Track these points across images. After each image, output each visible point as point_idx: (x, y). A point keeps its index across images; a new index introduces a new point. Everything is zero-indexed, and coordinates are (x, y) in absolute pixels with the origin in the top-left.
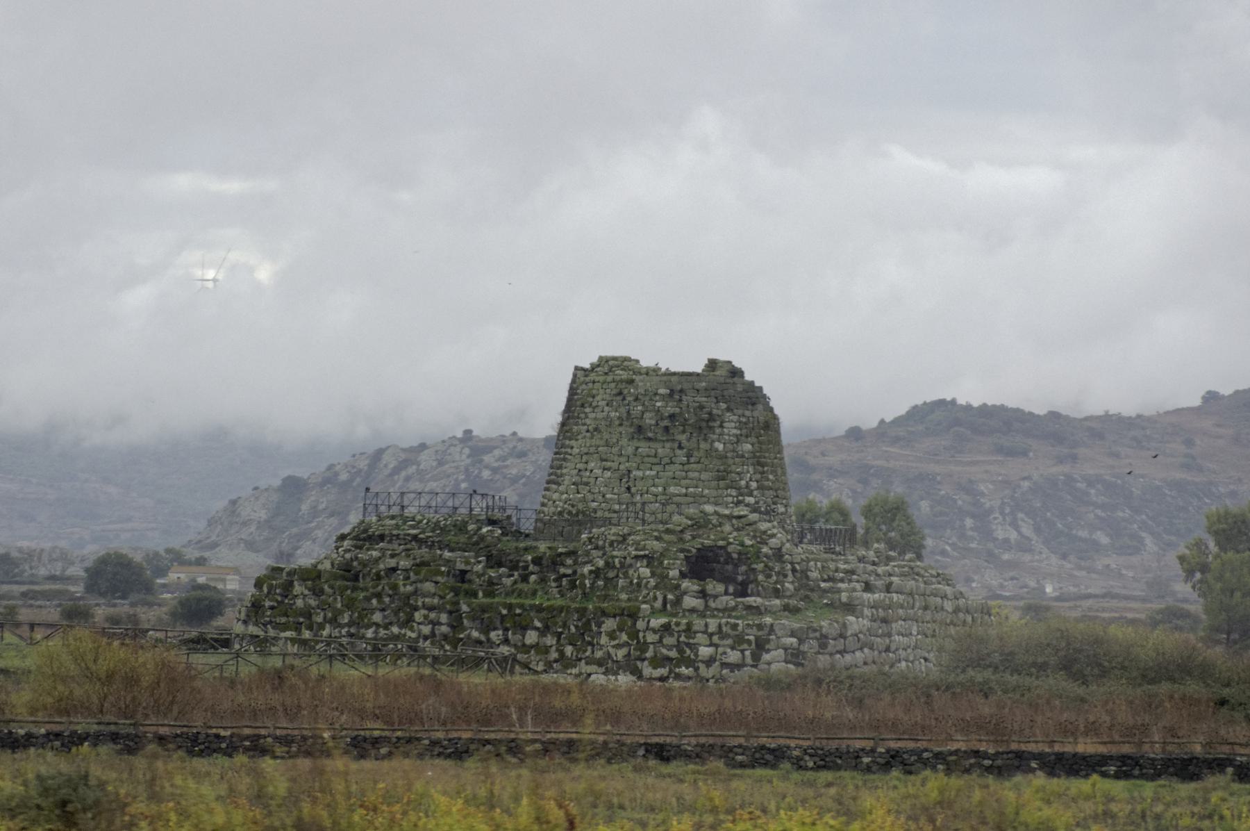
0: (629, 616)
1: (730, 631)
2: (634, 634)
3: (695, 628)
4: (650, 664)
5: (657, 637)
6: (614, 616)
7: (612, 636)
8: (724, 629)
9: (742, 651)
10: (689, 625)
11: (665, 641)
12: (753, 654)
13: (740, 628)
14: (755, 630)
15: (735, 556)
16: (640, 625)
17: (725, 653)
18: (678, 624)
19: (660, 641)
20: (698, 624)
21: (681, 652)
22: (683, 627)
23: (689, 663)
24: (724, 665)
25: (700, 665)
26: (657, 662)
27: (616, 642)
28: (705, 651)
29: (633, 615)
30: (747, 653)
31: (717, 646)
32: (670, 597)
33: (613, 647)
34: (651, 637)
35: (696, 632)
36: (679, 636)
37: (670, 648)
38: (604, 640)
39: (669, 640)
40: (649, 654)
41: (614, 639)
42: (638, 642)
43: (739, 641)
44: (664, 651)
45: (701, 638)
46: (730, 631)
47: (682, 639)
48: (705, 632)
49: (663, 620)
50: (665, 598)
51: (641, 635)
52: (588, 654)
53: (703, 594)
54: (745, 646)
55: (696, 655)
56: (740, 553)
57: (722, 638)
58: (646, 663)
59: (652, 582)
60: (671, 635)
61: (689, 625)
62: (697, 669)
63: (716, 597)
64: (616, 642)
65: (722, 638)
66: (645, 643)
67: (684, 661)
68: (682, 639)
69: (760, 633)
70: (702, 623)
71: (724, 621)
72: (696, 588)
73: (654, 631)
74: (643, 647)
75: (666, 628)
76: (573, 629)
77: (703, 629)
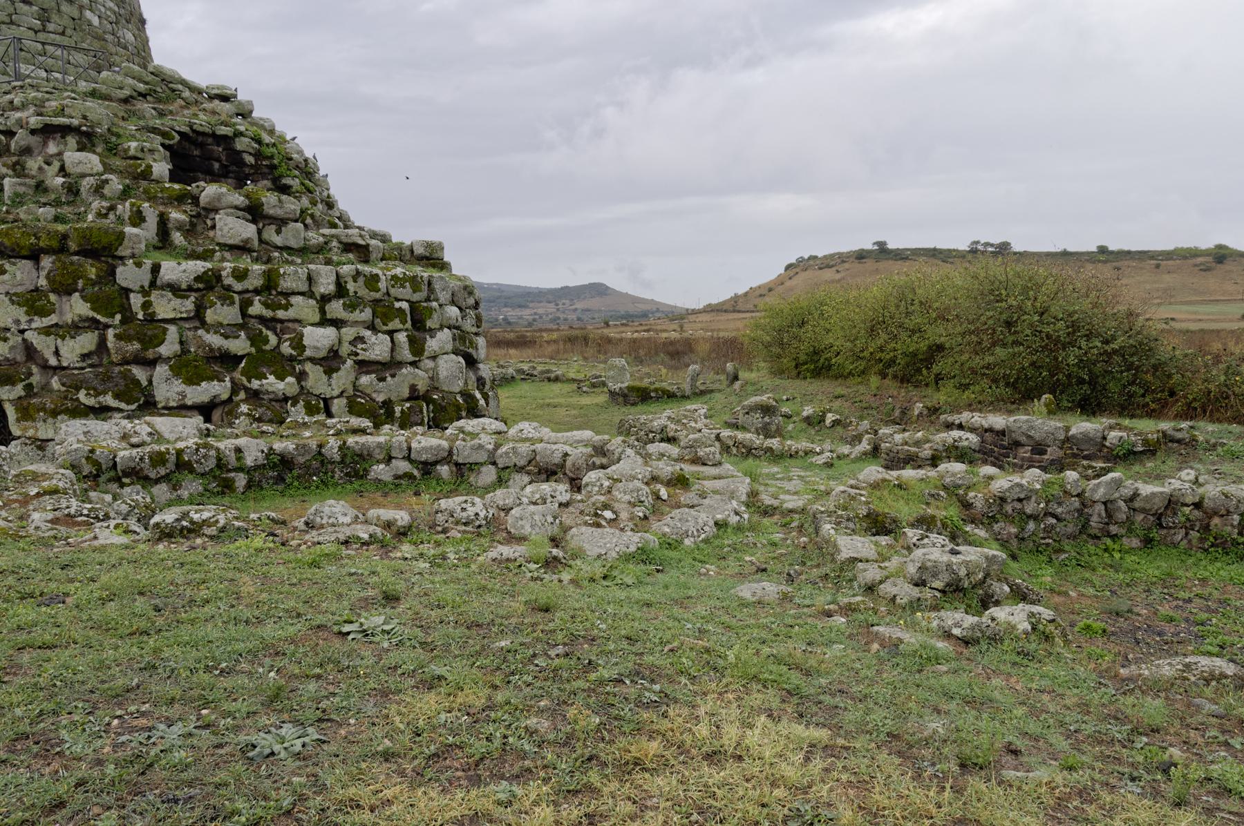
1: (363, 292)
2: (112, 299)
3: (286, 284)
5: (189, 304)
6: (34, 256)
8: (351, 287)
9: (391, 333)
11: (210, 316)
12: (411, 340)
13: (382, 285)
14: (406, 292)
15: (250, 159)
16: (128, 275)
17: (361, 339)
18: (240, 275)
20: (292, 275)
21: (257, 340)
22: (254, 282)
23: (283, 365)
24: (364, 366)
25: (308, 367)
26: (190, 367)
27: (53, 319)
28: (318, 338)
29: (104, 251)
30: (402, 337)
31: (337, 323)
32: (176, 215)
33: (46, 331)
34: (165, 307)
35: (287, 295)
36: (245, 305)
37: (229, 332)
40: (168, 348)
41: (43, 313)
42: (128, 317)
43: (383, 311)
44: (215, 340)
45: (303, 308)
46: (363, 292)
47: (257, 308)
48: (309, 294)
49: (199, 266)
50: (163, 221)
51: (136, 301)
53: (254, 212)
54: (395, 324)
55: (299, 345)
56: (258, 155)
57: (351, 307)
58: (161, 370)
59: (115, 184)
60: (226, 299)
62: (301, 377)
63: (281, 223)
64: (53, 319)
66: (151, 319)
68: (257, 308)
69: (416, 297)
70: (302, 272)
71: (346, 269)
72: (239, 199)
73: (176, 290)
74: (149, 330)
75: (209, 283)
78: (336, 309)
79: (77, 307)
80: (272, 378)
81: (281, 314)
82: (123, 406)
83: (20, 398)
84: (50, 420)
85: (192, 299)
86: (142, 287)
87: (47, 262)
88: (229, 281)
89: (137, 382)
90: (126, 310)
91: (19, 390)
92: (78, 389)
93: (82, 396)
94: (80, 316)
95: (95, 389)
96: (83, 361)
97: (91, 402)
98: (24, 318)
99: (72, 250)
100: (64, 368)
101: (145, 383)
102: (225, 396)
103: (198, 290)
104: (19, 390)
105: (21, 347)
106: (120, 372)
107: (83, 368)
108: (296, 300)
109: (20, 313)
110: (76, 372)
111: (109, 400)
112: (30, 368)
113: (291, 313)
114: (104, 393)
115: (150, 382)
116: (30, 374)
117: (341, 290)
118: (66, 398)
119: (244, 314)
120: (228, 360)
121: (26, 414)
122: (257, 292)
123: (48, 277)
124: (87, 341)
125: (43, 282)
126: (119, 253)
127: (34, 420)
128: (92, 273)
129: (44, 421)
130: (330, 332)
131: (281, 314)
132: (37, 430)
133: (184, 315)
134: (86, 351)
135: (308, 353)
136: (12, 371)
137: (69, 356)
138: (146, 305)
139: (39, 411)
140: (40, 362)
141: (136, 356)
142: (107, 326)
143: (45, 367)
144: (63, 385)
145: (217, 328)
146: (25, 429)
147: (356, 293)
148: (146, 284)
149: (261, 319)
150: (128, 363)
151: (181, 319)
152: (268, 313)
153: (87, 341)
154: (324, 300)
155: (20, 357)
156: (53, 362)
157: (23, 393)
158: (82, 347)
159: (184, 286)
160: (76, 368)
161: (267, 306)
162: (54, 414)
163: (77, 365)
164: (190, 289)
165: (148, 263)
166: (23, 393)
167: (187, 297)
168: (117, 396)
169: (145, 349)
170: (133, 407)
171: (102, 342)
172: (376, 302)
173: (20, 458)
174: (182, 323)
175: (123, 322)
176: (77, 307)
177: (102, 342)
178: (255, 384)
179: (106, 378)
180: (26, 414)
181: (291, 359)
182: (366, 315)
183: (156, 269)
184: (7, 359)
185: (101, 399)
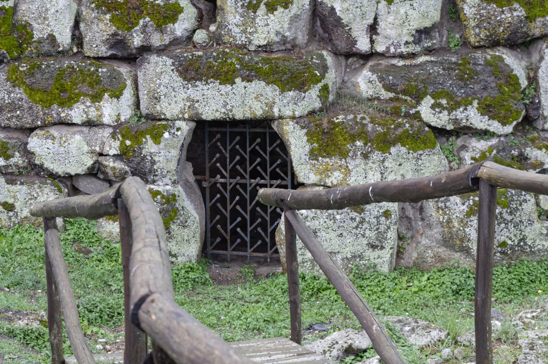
52: (180, 27)
82: (495, 126)
83: (312, 113)
84: (376, 156)
89: (511, 80)
91: (312, 99)
92: (419, 99)
93: (425, 109)
95: (449, 96)
96: (418, 41)
97: (441, 120)
100: (382, 55)
101: (524, 83)
104: (312, 99)
105: (306, 16)
106: (487, 63)
107: (413, 56)
110: (401, 63)
111: (474, 117)
112: (321, 57)
114: (467, 104)
115: (533, 80)
116: (325, 69)
118: (396, 113)
121: (328, 141)
127: (344, 155)
129: (366, 156)
132: (348, 172)
134: (428, 24)
136: (293, 64)
137: (392, 33)
139: (353, 138)
140: (342, 45)
141: (514, 33)
143: (352, 57)
144: (388, 88)
146: (327, 172)
150: (494, 44)
155: (302, 38)
156: (363, 44)
157: (317, 105)
158: (424, 16)
160: (402, 56)
162: (385, 143)
163: (404, 50)
166: (317, 105)
168: (487, 110)
169: (529, 19)
170: (509, 129)
179: (466, 75)
180: (328, 141)
184: (284, 40)
185: (459, 114)
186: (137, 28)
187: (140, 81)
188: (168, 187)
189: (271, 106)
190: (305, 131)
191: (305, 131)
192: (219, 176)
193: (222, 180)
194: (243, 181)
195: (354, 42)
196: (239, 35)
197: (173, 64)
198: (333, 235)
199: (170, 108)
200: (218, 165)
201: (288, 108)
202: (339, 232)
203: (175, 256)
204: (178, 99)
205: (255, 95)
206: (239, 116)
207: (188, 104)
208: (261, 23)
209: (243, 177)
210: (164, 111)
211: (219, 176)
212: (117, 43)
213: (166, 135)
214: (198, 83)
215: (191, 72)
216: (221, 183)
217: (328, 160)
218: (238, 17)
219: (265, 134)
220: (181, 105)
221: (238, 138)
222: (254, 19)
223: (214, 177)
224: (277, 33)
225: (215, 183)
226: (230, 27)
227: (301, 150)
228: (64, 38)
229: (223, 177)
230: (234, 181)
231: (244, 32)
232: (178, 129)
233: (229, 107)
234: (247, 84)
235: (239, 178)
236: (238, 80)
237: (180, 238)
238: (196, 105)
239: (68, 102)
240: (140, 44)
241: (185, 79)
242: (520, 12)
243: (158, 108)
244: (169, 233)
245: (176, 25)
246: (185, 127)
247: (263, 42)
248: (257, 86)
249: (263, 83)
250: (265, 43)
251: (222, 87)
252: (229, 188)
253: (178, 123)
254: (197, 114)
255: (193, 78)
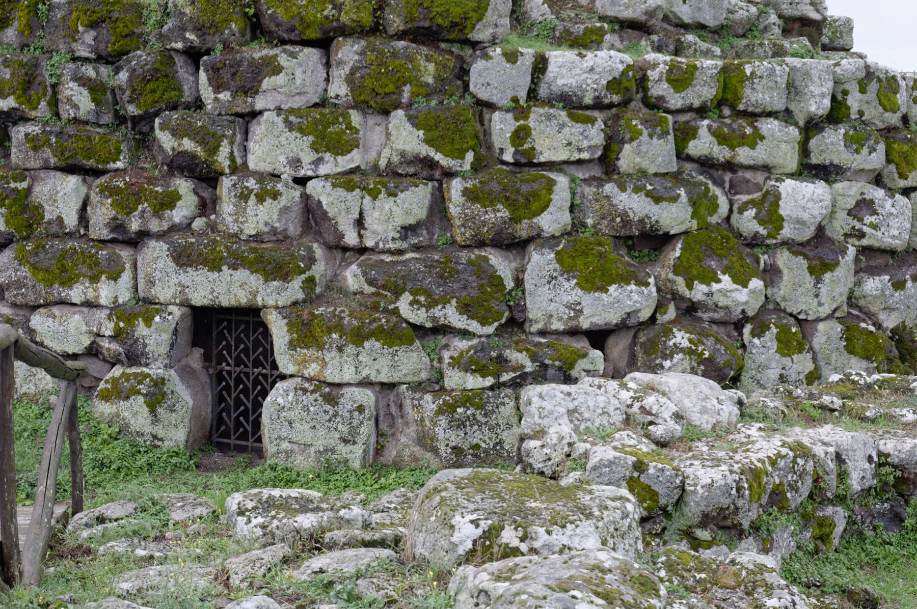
0: (424, 35)
1: (876, 115)
2: (458, 120)
3: (757, 96)
4: (567, 265)
5: (595, 135)
7: (322, 124)
8: (854, 101)
10: (730, 83)
16: (493, 77)
19: (606, 162)
21: (701, 203)
22: (704, 91)
23: (747, 254)
24: (874, 259)
25: (783, 259)
27: (354, 159)
35: (752, 116)
36: (685, 134)
37: (660, 188)
38: (271, 146)
39: (649, 152)
40: (553, 220)
41: (340, 147)
44: (634, 204)
45: (778, 143)
47: (703, 143)
48: (787, 116)
51: (501, 126)
52: (178, 214)
55: (770, 214)
57: (855, 142)
58: (540, 261)
61: (730, 83)
62: (771, 274)
64: (354, 159)
65: (855, 142)
66: (526, 162)
67: (724, 247)
76: (80, 101)
77: (779, 104)
78: (831, 145)
79: (403, 137)
80: (726, 279)
81: (744, 155)
82: (474, 326)
83: (295, 304)
84: (350, 349)
85: (600, 124)
86: (515, 100)
87: (348, 52)
88: (659, 89)
89: (497, 282)
90: (483, 142)
91: (294, 290)
92: (397, 294)
93: (404, 305)
94: (403, 154)
95: (428, 293)
96: (404, 238)
97: (419, 317)
98: (308, 157)
99: (392, 31)
100: (372, 250)
101: (510, 284)
102: (645, 315)
103: (611, 106)
104: (294, 290)
105: (297, 209)
106: (470, 263)
107: (400, 252)
108: (769, 126)
109: (301, 147)
110: (388, 258)
111: (451, 315)
112: (310, 250)
113: (759, 154)
114: (445, 302)
115: (519, 282)
116: (312, 260)
117: (837, 113)
118: (375, 307)
119: (681, 155)
120: (654, 241)
121: (306, 334)
122: (702, 111)
123: (350, 79)
124: (414, 202)
125: (339, 89)
126: (475, 36)
127: (321, 347)
128: (429, 72)
129: (340, 349)
130: (817, 190)
131: (744, 155)
132: (324, 364)
133: (585, 156)
134: (412, 221)
135: (787, 232)
136: (281, 254)
137: (379, 228)
138: (520, 135)
139: (330, 331)
140: (330, 238)
141: (499, 233)
142: (449, 174)
143: (338, 248)
144: (371, 283)
145: (638, 180)
146: (304, 363)
147: (861, 113)
148: (522, 95)
149: (706, 164)
150: (481, 244)
151: (579, 162)
152: (721, 153)
153: (414, 202)
154: (812, 127)
155: (294, 229)
156: (351, 238)
157: (300, 296)
158: (408, 213)
159: (588, 100)
160: (390, 252)
161: (721, 138)
162: (359, 337)
163: (392, 246)
164: (598, 105)
165: (528, 53)
166: (300, 296)
167: (592, 121)
168: (465, 309)
169: (515, 220)
170: (490, 330)
171: (439, 203)
172: (888, 132)
173: (291, 415)
174: (572, 170)
175: (477, 167)
176: (403, 137)
177: (439, 203)
178: (699, 292)
179: (447, 273)
180: (306, 334)
181: (754, 242)
182: (876, 159)
183: (540, 66)
184: (274, 231)
185: (437, 311)
186: (136, 213)
187: (139, 265)
188: (160, 371)
189: (254, 294)
190: (286, 321)
191: (286, 321)
192: (224, 364)
193: (228, 368)
194: (246, 370)
195: (342, 236)
196: (231, 224)
197: (169, 250)
198: (306, 427)
199: (164, 292)
200: (225, 352)
201: (273, 296)
202: (312, 424)
203: (161, 440)
204: (171, 284)
205: (240, 283)
206: (225, 303)
207: (179, 289)
208: (251, 213)
209: (246, 366)
210: (158, 295)
211: (224, 364)
212: (117, 226)
213: (157, 319)
214: (189, 269)
215: (184, 258)
216: (227, 371)
217: (306, 351)
218: (231, 206)
219: (231, 320)
220: (173, 290)
221: (243, 327)
222: (245, 209)
223: (221, 364)
224: (266, 224)
225: (222, 371)
226: (224, 216)
227: (282, 340)
228: (71, 220)
229: (228, 365)
230: (238, 369)
231: (236, 221)
232: (170, 314)
233: (215, 294)
234: (233, 272)
235: (242, 366)
236: (225, 268)
237: (166, 423)
238: (187, 290)
239: (69, 282)
240: (138, 228)
241: (177, 264)
242: (503, 213)
243: (153, 292)
244: (156, 416)
245: (174, 212)
246: (177, 311)
247: (253, 232)
248: (242, 274)
249: (248, 272)
250: (254, 233)
251: (210, 274)
252: (233, 376)
253: (171, 308)
254: (187, 299)
255: (184, 264)
